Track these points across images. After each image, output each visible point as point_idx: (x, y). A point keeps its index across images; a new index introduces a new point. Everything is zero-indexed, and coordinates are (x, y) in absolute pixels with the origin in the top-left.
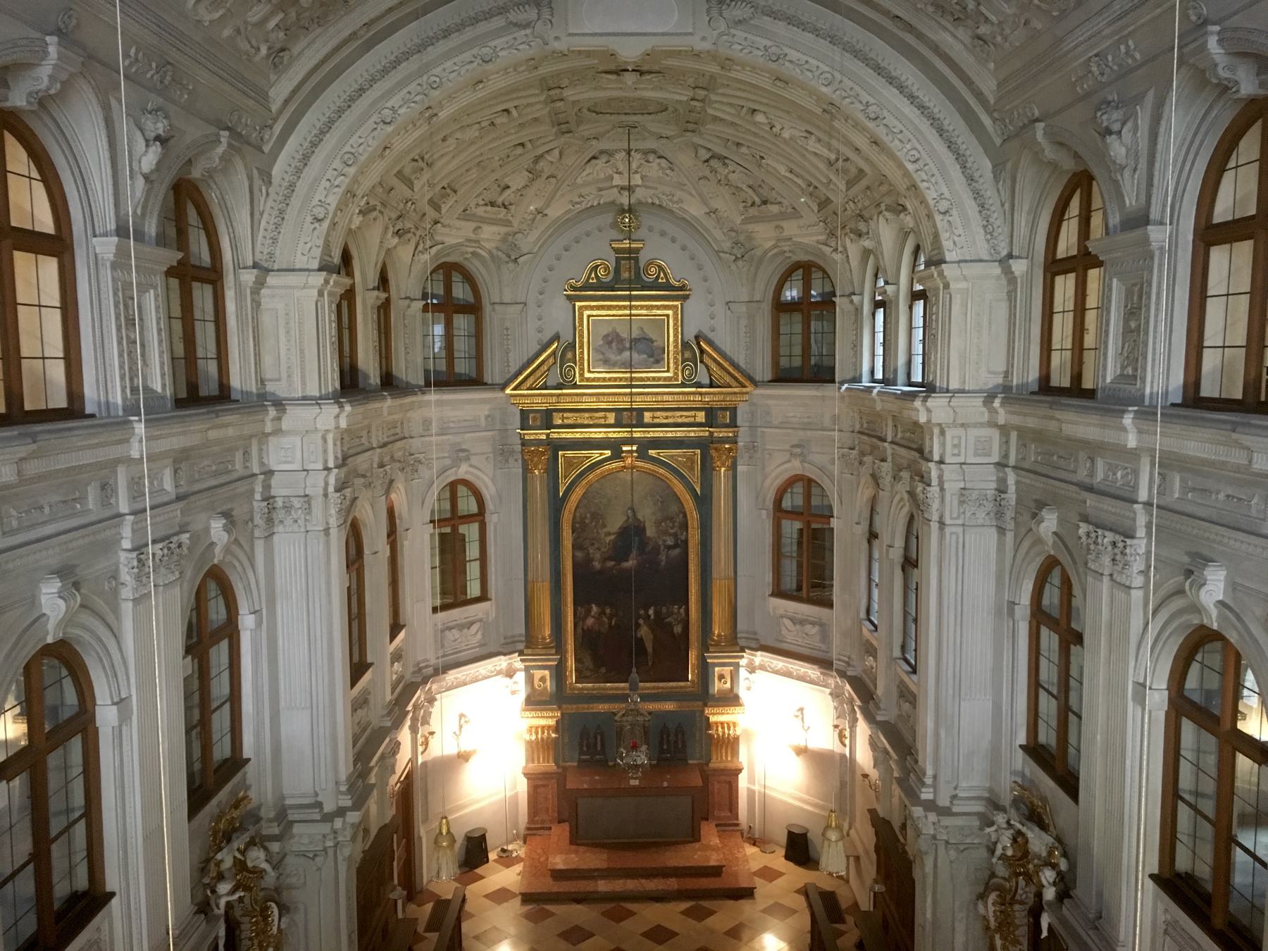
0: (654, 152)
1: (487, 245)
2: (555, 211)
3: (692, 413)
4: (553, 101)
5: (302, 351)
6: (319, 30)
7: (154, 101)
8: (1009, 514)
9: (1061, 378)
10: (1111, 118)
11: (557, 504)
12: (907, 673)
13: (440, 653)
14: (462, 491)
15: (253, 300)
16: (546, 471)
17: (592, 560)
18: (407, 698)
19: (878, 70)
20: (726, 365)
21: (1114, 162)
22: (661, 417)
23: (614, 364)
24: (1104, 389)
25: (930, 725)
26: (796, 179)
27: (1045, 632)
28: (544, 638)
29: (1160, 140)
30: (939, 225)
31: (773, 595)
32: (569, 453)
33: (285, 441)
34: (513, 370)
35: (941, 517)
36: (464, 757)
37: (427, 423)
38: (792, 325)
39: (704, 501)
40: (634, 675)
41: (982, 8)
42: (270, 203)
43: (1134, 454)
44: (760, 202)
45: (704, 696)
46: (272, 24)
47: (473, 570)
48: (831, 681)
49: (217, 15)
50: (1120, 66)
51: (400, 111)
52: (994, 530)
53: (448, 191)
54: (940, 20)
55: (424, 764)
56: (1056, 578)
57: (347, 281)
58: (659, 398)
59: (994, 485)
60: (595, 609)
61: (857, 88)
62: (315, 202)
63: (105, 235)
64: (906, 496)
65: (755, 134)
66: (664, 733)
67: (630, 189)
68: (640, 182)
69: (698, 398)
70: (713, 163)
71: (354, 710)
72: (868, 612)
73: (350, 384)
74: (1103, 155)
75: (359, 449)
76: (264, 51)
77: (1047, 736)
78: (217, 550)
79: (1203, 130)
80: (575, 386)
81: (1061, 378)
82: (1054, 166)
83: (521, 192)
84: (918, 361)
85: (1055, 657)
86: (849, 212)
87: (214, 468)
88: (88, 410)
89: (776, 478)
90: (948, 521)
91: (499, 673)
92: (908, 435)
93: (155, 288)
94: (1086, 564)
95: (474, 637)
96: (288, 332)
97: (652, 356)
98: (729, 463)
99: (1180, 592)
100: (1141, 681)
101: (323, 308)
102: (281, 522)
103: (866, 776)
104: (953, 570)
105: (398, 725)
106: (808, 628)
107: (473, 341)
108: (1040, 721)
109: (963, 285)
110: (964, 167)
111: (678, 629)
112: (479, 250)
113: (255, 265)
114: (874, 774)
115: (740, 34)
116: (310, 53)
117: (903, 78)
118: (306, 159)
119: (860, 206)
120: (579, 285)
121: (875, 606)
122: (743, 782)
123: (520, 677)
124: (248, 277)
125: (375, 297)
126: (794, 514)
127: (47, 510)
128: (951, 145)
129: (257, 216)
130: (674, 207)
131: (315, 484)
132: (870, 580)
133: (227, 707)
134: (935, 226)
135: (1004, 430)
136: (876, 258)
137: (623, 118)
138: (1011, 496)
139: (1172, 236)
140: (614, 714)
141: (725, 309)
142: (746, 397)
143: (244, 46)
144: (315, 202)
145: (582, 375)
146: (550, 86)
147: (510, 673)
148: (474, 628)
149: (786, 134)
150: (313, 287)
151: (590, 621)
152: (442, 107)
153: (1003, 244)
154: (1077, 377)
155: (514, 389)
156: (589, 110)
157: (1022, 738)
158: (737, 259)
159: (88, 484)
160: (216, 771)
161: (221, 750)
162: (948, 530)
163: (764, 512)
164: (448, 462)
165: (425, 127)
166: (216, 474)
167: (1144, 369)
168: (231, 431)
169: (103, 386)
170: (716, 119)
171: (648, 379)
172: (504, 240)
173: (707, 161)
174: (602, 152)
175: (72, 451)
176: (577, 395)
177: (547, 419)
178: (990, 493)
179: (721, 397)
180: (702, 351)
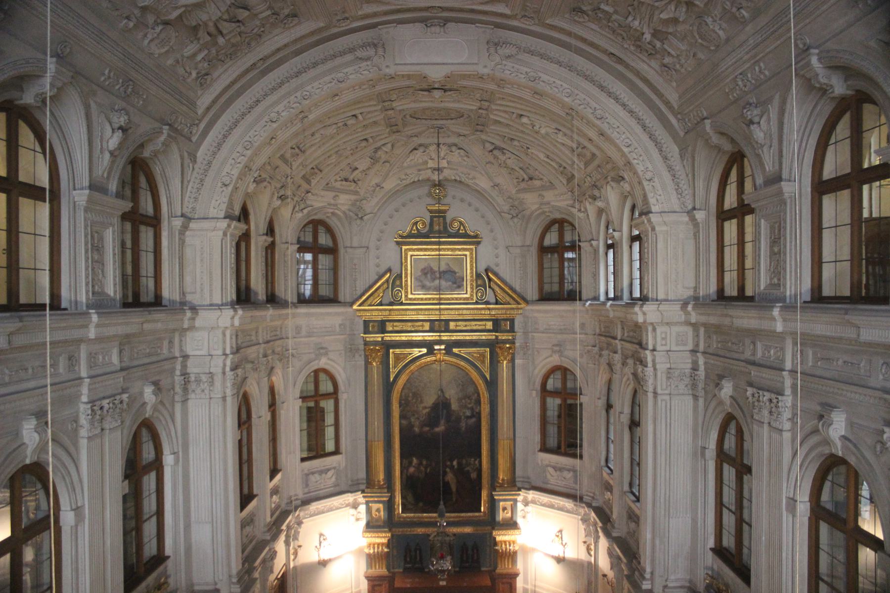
0: (455, 145)
1: (344, 208)
2: (390, 184)
3: (483, 323)
4: (386, 110)
5: (211, 273)
6: (231, 63)
7: (120, 104)
8: (701, 385)
9: (731, 290)
10: (753, 113)
11: (388, 387)
12: (634, 502)
13: (306, 490)
14: (322, 376)
15: (180, 239)
16: (381, 363)
17: (413, 426)
18: (281, 520)
19: (602, 88)
20: (507, 289)
21: (757, 142)
22: (462, 325)
24: (759, 295)
25: (649, 536)
26: (552, 163)
27: (726, 467)
28: (379, 481)
29: (785, 126)
30: (647, 188)
31: (541, 450)
32: (398, 351)
33: (198, 335)
34: (359, 293)
35: (655, 389)
36: (323, 563)
37: (298, 329)
38: (551, 261)
39: (492, 384)
40: (442, 506)
41: (666, 46)
42: (195, 174)
43: (781, 337)
44: (528, 179)
45: (492, 522)
46: (199, 57)
47: (330, 432)
48: (582, 511)
49: (163, 50)
50: (756, 80)
51: (283, 114)
52: (691, 397)
53: (316, 170)
54: (640, 56)
55: (295, 568)
56: (732, 429)
57: (245, 227)
58: (461, 312)
59: (689, 366)
60: (415, 461)
61: (587, 98)
62: (224, 173)
63: (82, 189)
64: (631, 377)
65: (522, 132)
66: (464, 549)
67: (439, 170)
68: (446, 165)
69: (487, 312)
70: (496, 152)
71: (243, 526)
72: (607, 460)
73: (244, 297)
74: (749, 138)
75: (249, 344)
76: (194, 75)
77: (728, 541)
78: (148, 408)
79: (812, 120)
80: (402, 304)
81: (731, 290)
82: (719, 149)
83: (365, 172)
84: (637, 282)
85: (733, 485)
86: (587, 184)
87: (148, 351)
88: (63, 306)
89: (543, 367)
90: (659, 391)
91: (347, 505)
92: (631, 334)
93: (113, 226)
94: (752, 417)
95: (330, 479)
96: (202, 260)
97: (455, 283)
98: (509, 358)
99: (816, 431)
100: (791, 496)
101: (226, 243)
102: (194, 391)
103: (605, 576)
104: (664, 427)
105: (275, 537)
106: (565, 474)
107: (332, 273)
108: (724, 531)
110: (660, 150)
111: (474, 475)
112: (336, 211)
113: (183, 215)
114: (611, 574)
115: (509, 64)
116: (224, 76)
117: (618, 93)
118: (219, 146)
119: (594, 179)
120: (405, 234)
121: (612, 456)
122: (520, 583)
123: (363, 508)
124: (178, 223)
125: (264, 240)
126: (555, 393)
127: (30, 371)
128: (651, 137)
129: (185, 183)
130: (470, 182)
131: (216, 365)
132: (608, 438)
133: (154, 519)
134: (644, 189)
135: (695, 326)
136: (607, 214)
137: (435, 122)
138: (701, 373)
139: (798, 187)
140: (429, 535)
141: (505, 252)
142: (520, 311)
143: (181, 71)
144: (224, 173)
145: (406, 296)
146: (383, 99)
147: (355, 506)
148: (330, 474)
149: (543, 131)
150: (220, 230)
151: (412, 470)
152: (310, 111)
153: (689, 201)
154: (742, 288)
155: (360, 305)
156: (411, 116)
157: (711, 543)
158: (513, 217)
159: (60, 355)
160: (145, 564)
161: (150, 549)
162: (659, 398)
163: (534, 392)
164: (313, 356)
165: (299, 125)
166: (150, 355)
167: (785, 278)
168: (159, 325)
169: (75, 289)
170: (497, 122)
171: (453, 299)
172: (354, 205)
173: (491, 151)
174: (420, 145)
175: (48, 328)
176: (403, 310)
177: (382, 327)
178: (688, 371)
180: (490, 280)
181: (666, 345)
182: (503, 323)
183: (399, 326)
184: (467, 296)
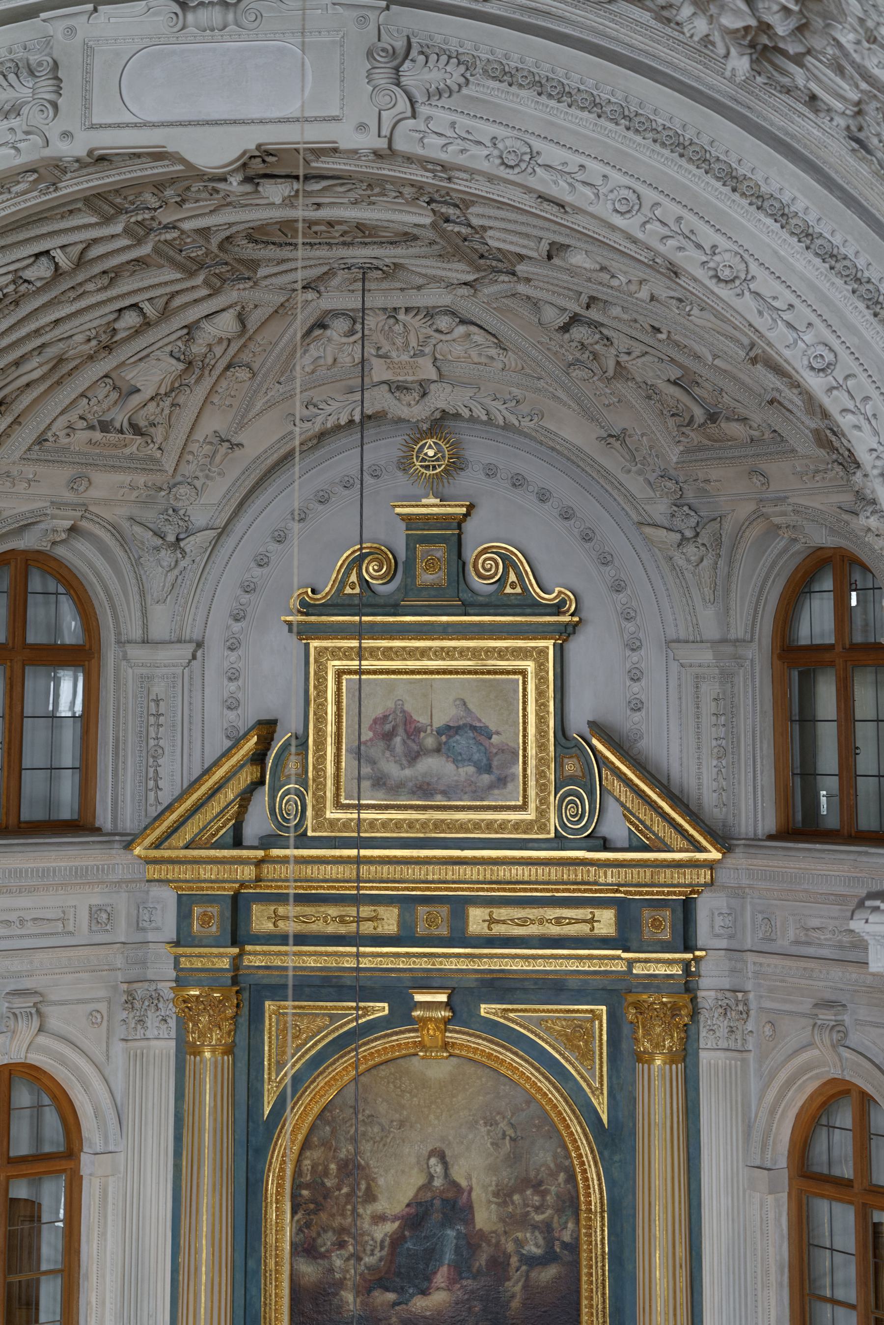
22: (510, 921)
23: (396, 789)
58: (503, 873)
80: (303, 841)
97: (488, 769)
171: (476, 826)
179: (645, 875)
182: (646, 913)
183: (292, 919)
184: (530, 815)
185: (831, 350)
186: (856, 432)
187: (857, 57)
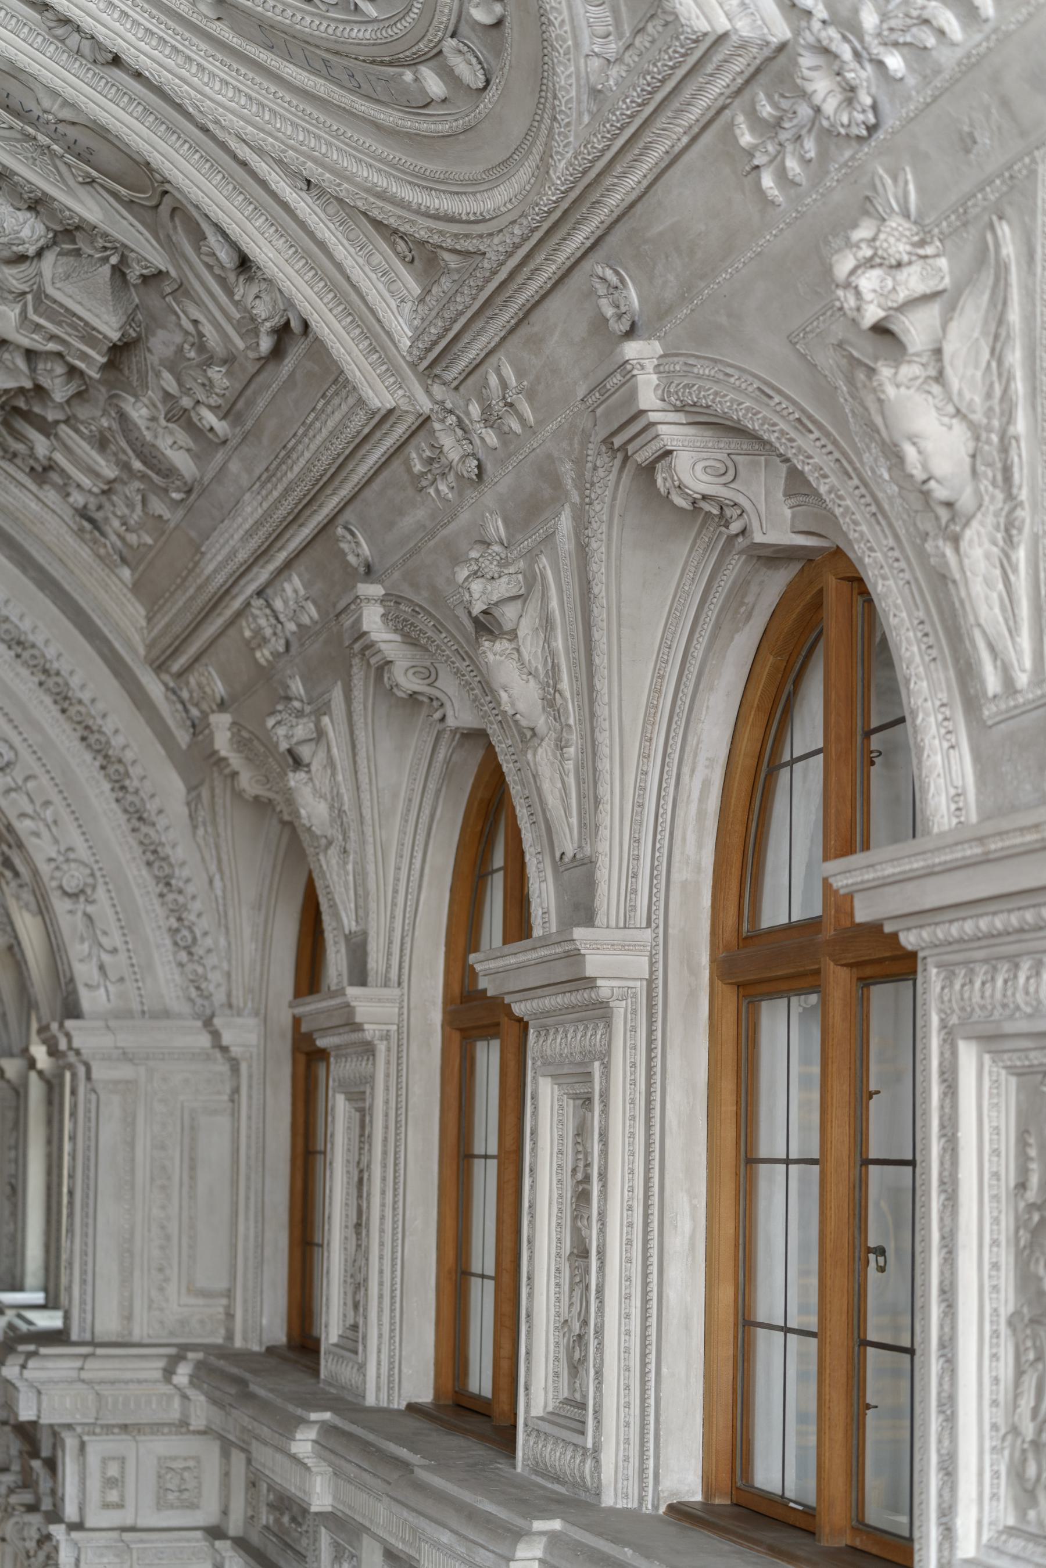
109: (125, 1072)
128: (88, 734)
153: (216, 977)
181: (120, 1506)
185: (12, 747)
186: (34, 840)
187: (148, 436)
